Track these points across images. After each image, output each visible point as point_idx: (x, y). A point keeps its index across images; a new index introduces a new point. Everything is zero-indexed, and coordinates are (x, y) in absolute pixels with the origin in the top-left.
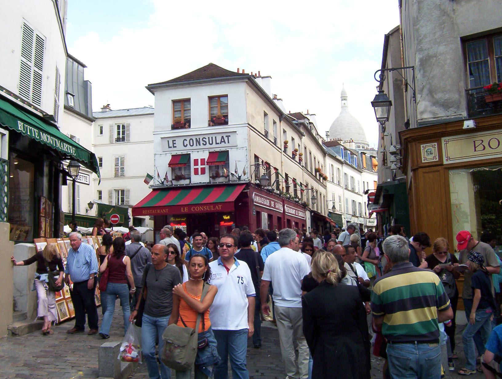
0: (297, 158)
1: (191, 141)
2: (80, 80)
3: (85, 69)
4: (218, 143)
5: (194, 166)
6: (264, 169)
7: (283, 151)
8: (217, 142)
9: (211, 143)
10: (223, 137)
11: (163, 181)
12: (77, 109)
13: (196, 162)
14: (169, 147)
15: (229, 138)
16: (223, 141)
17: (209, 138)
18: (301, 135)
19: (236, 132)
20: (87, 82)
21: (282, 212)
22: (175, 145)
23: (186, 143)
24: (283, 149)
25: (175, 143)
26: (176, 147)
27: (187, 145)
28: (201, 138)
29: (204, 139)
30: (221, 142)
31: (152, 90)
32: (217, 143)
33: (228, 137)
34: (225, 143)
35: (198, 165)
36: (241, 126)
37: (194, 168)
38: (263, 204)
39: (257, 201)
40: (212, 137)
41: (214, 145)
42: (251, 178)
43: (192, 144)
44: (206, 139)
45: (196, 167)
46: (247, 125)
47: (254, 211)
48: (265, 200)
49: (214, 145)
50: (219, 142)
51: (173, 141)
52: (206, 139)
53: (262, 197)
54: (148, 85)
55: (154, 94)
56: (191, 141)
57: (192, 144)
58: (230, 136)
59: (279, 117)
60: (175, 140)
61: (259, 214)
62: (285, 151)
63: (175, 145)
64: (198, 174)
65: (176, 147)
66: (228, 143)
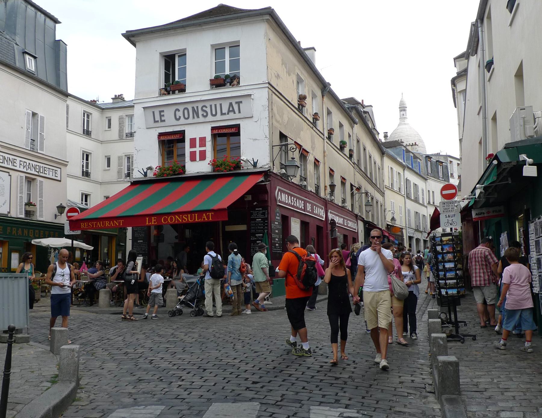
0: (347, 151)
1: (186, 111)
2: (49, 41)
3: (57, 25)
4: (225, 114)
5: (191, 148)
6: (293, 152)
7: (326, 137)
8: (223, 112)
9: (214, 113)
10: (231, 104)
11: (145, 171)
12: (42, 77)
13: (193, 142)
14: (155, 122)
15: (241, 104)
16: (231, 110)
17: (211, 106)
18: (352, 122)
19: (250, 95)
20: (60, 42)
21: (324, 219)
22: (163, 119)
24: (326, 135)
25: (163, 116)
26: (164, 121)
27: (180, 117)
28: (200, 105)
29: (204, 108)
30: (229, 111)
31: (132, 39)
32: (222, 114)
34: (235, 113)
35: (195, 147)
36: (258, 86)
38: (293, 206)
39: (283, 199)
40: (216, 105)
41: (219, 117)
42: (274, 165)
43: (186, 116)
44: (206, 107)
45: (193, 150)
46: (267, 85)
47: (278, 215)
48: (296, 201)
49: (219, 117)
51: (160, 112)
52: (206, 107)
53: (292, 196)
54: (127, 31)
55: (134, 45)
56: (186, 111)
57: (186, 116)
58: (241, 102)
59: (322, 90)
60: (163, 111)
61: (285, 221)
62: (329, 138)
65: (164, 121)
66: (239, 112)
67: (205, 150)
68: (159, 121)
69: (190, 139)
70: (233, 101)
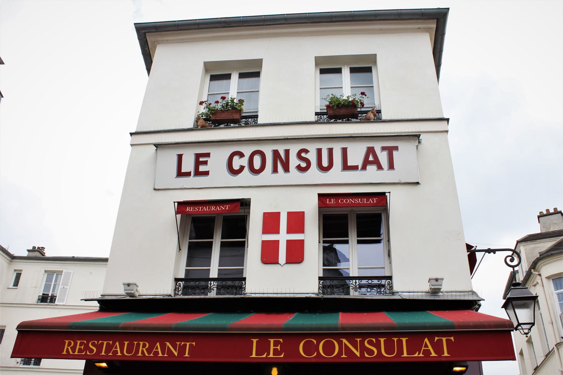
10: (371, 150)
14: (180, 174)
15: (395, 153)
19: (416, 137)
22: (202, 168)
23: (237, 163)
27: (242, 168)
28: (294, 149)
33: (390, 150)
37: (263, 242)
40: (330, 151)
50: (360, 164)
58: (396, 148)
63: (202, 168)
64: (277, 263)
67: (303, 241)
68: (192, 174)
69: (265, 214)
70: (377, 146)
